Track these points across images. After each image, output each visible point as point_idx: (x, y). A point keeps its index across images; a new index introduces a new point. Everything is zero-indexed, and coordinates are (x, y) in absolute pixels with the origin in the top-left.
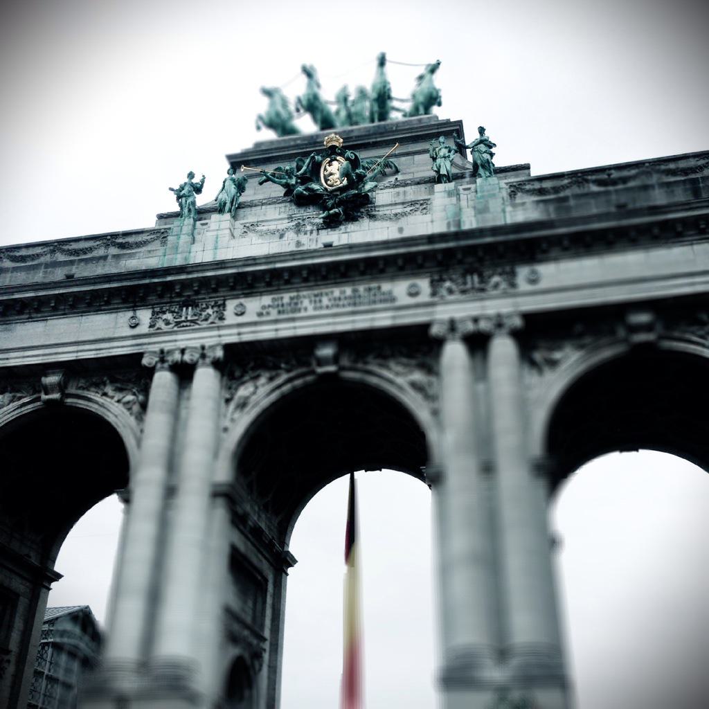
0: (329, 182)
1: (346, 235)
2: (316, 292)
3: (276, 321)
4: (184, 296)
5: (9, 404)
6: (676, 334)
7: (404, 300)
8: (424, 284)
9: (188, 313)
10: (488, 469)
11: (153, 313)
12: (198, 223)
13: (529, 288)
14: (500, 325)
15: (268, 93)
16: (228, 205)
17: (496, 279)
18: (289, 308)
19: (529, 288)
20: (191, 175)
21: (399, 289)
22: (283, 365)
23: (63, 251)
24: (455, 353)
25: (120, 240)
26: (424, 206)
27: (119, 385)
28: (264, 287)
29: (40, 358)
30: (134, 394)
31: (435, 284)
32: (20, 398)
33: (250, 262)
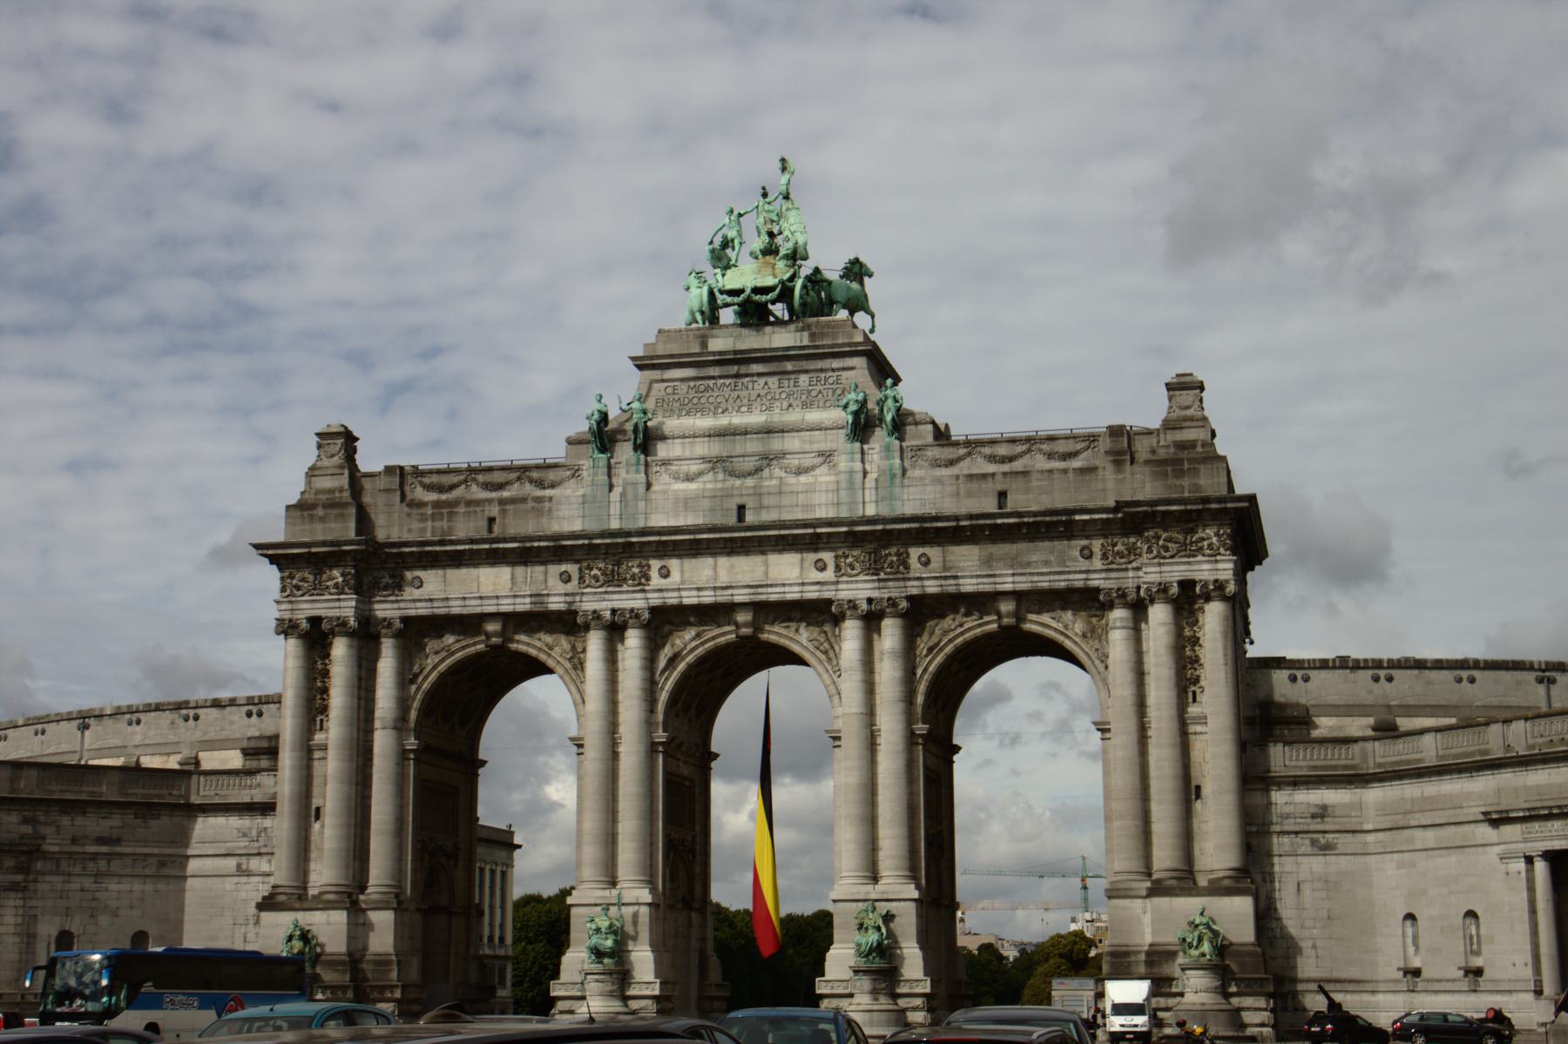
25: (535, 475)
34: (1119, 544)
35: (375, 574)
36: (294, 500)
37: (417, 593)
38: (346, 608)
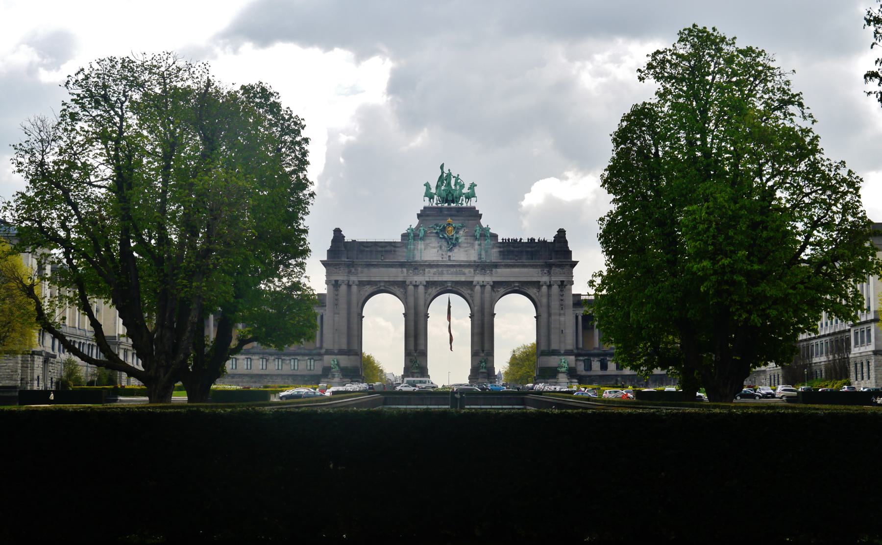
8: (472, 270)
15: (425, 185)
20: (411, 226)
21: (467, 270)
24: (478, 288)
25: (393, 244)
36: (328, 248)
38: (345, 278)
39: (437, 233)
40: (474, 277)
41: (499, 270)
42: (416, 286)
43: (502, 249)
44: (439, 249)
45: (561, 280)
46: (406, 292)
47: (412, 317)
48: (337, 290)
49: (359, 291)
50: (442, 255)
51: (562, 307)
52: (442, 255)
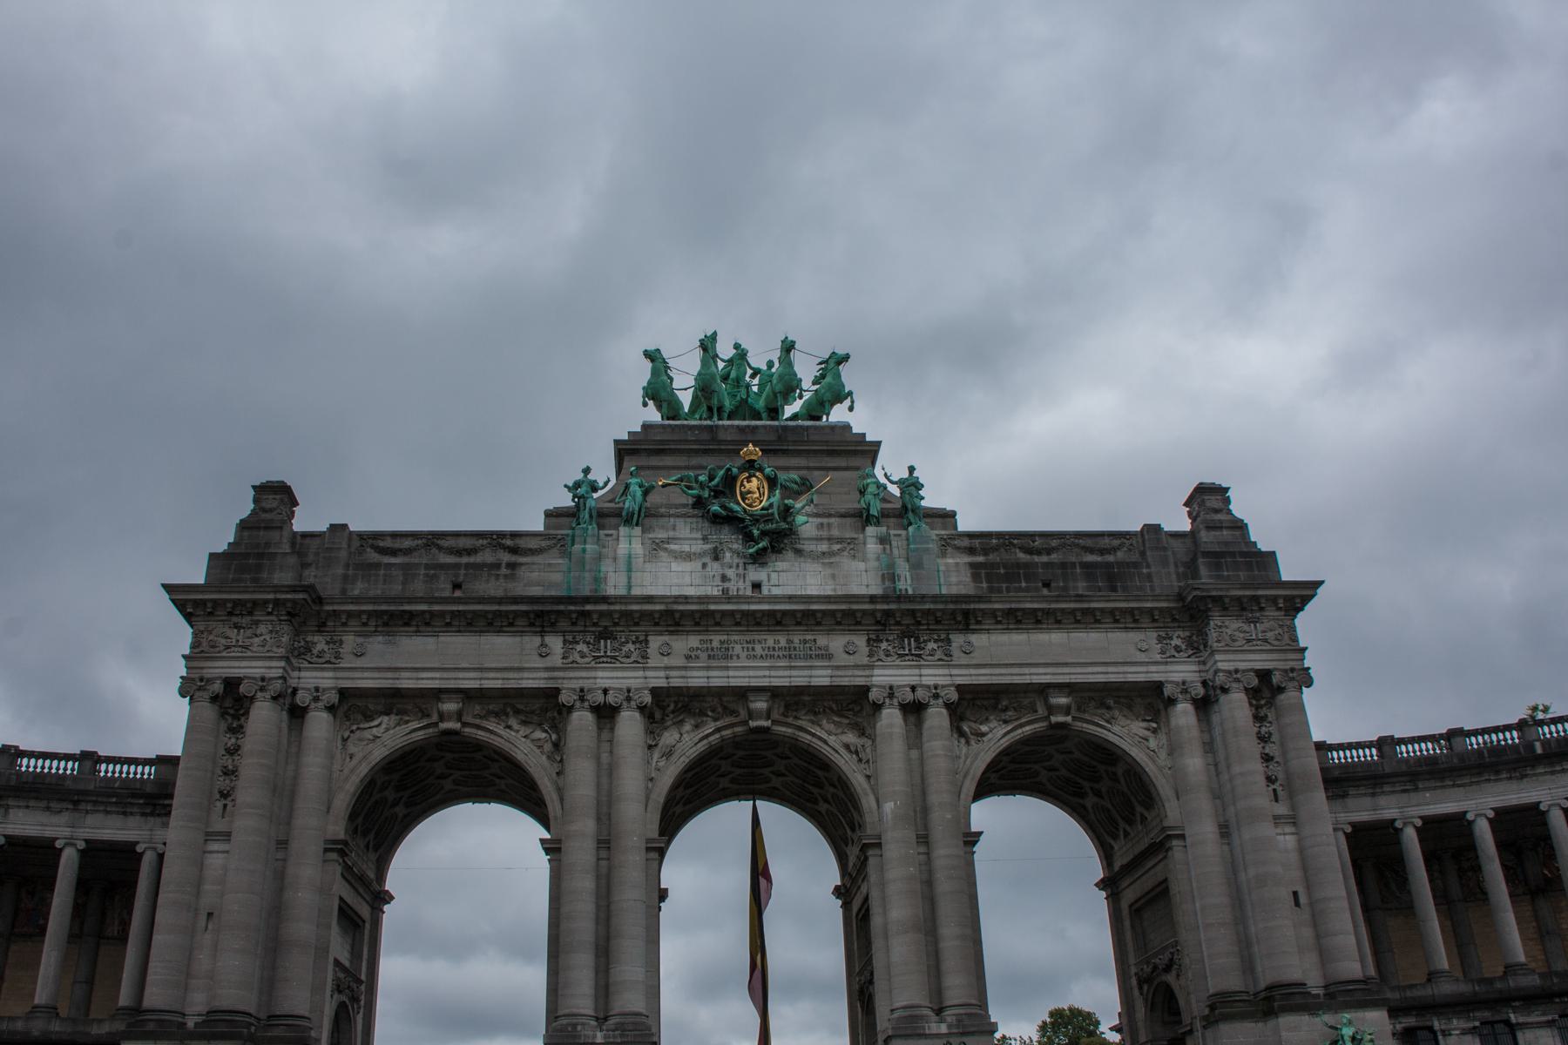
0: (747, 501)
1: (776, 574)
2: (748, 638)
3: (708, 668)
4: (600, 626)
5: (395, 727)
6: (1087, 716)
7: (843, 659)
8: (860, 641)
9: (607, 646)
10: (924, 839)
11: (565, 642)
12: (601, 532)
13: (964, 660)
14: (936, 696)
15: (647, 354)
16: (636, 516)
17: (931, 645)
18: (720, 654)
19: (964, 660)
20: (587, 471)
21: (836, 643)
22: (710, 714)
23: (440, 548)
24: (891, 718)
25: (509, 542)
26: (852, 546)
27: (523, 718)
28: (691, 626)
29: (437, 682)
30: (546, 731)
31: (872, 642)
32: (407, 722)
33: (680, 600)
34: (1174, 637)
35: (309, 638)
36: (221, 547)
37: (359, 663)
38: (274, 669)
39: (699, 503)
40: (872, 667)
41: (978, 640)
42: (606, 714)
43: (981, 559)
44: (707, 560)
45: (1259, 666)
46: (556, 745)
47: (582, 852)
48: (237, 730)
49: (345, 740)
50: (724, 578)
51: (1281, 784)
52: (724, 578)
